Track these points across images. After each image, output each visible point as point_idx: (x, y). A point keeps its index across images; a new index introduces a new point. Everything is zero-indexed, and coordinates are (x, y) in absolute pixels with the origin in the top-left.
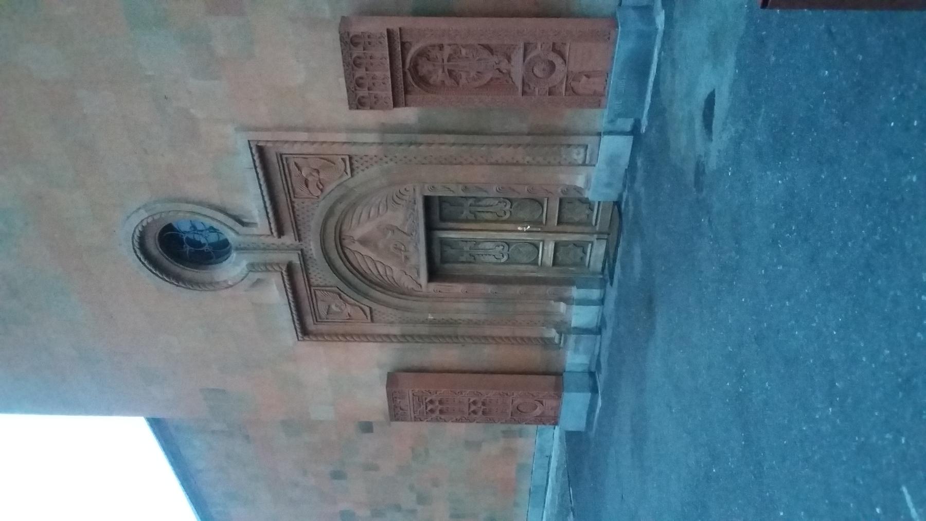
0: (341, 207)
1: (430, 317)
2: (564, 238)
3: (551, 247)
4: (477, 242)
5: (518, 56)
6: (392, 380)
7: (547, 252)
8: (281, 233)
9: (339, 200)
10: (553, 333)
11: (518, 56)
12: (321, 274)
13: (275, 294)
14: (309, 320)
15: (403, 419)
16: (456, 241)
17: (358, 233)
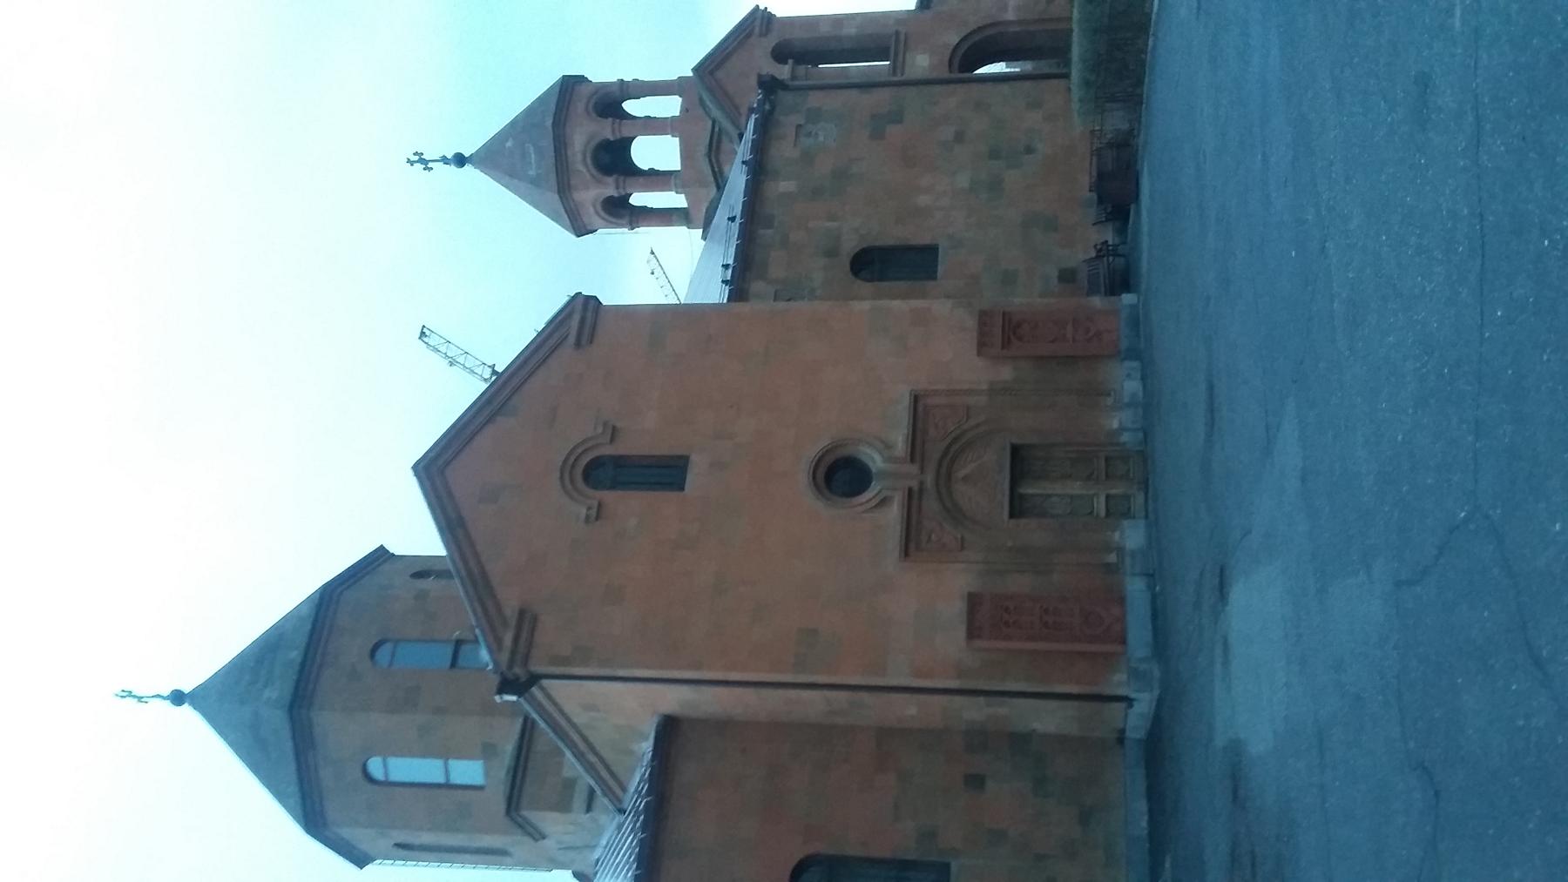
0: (955, 447)
1: (1010, 544)
2: (1113, 492)
3: (1103, 499)
4: (1050, 496)
5: (1069, 328)
6: (973, 601)
7: (1100, 506)
8: (912, 460)
9: (956, 440)
10: (1112, 558)
11: (1069, 328)
12: (931, 505)
13: (894, 512)
14: (912, 546)
15: (979, 637)
16: (1033, 495)
17: (962, 473)
